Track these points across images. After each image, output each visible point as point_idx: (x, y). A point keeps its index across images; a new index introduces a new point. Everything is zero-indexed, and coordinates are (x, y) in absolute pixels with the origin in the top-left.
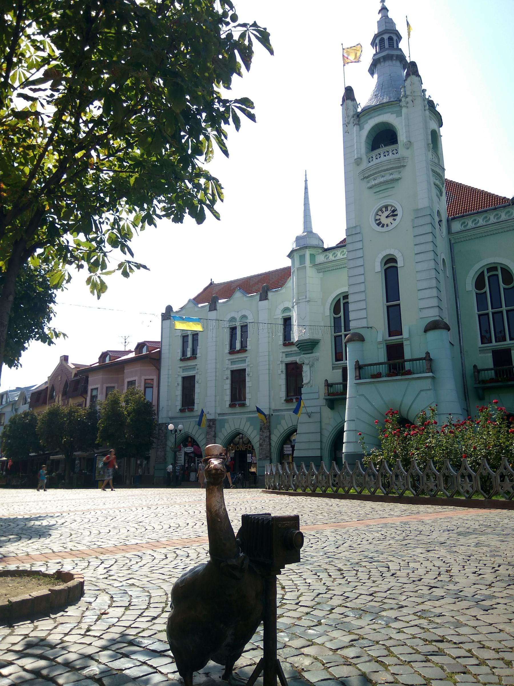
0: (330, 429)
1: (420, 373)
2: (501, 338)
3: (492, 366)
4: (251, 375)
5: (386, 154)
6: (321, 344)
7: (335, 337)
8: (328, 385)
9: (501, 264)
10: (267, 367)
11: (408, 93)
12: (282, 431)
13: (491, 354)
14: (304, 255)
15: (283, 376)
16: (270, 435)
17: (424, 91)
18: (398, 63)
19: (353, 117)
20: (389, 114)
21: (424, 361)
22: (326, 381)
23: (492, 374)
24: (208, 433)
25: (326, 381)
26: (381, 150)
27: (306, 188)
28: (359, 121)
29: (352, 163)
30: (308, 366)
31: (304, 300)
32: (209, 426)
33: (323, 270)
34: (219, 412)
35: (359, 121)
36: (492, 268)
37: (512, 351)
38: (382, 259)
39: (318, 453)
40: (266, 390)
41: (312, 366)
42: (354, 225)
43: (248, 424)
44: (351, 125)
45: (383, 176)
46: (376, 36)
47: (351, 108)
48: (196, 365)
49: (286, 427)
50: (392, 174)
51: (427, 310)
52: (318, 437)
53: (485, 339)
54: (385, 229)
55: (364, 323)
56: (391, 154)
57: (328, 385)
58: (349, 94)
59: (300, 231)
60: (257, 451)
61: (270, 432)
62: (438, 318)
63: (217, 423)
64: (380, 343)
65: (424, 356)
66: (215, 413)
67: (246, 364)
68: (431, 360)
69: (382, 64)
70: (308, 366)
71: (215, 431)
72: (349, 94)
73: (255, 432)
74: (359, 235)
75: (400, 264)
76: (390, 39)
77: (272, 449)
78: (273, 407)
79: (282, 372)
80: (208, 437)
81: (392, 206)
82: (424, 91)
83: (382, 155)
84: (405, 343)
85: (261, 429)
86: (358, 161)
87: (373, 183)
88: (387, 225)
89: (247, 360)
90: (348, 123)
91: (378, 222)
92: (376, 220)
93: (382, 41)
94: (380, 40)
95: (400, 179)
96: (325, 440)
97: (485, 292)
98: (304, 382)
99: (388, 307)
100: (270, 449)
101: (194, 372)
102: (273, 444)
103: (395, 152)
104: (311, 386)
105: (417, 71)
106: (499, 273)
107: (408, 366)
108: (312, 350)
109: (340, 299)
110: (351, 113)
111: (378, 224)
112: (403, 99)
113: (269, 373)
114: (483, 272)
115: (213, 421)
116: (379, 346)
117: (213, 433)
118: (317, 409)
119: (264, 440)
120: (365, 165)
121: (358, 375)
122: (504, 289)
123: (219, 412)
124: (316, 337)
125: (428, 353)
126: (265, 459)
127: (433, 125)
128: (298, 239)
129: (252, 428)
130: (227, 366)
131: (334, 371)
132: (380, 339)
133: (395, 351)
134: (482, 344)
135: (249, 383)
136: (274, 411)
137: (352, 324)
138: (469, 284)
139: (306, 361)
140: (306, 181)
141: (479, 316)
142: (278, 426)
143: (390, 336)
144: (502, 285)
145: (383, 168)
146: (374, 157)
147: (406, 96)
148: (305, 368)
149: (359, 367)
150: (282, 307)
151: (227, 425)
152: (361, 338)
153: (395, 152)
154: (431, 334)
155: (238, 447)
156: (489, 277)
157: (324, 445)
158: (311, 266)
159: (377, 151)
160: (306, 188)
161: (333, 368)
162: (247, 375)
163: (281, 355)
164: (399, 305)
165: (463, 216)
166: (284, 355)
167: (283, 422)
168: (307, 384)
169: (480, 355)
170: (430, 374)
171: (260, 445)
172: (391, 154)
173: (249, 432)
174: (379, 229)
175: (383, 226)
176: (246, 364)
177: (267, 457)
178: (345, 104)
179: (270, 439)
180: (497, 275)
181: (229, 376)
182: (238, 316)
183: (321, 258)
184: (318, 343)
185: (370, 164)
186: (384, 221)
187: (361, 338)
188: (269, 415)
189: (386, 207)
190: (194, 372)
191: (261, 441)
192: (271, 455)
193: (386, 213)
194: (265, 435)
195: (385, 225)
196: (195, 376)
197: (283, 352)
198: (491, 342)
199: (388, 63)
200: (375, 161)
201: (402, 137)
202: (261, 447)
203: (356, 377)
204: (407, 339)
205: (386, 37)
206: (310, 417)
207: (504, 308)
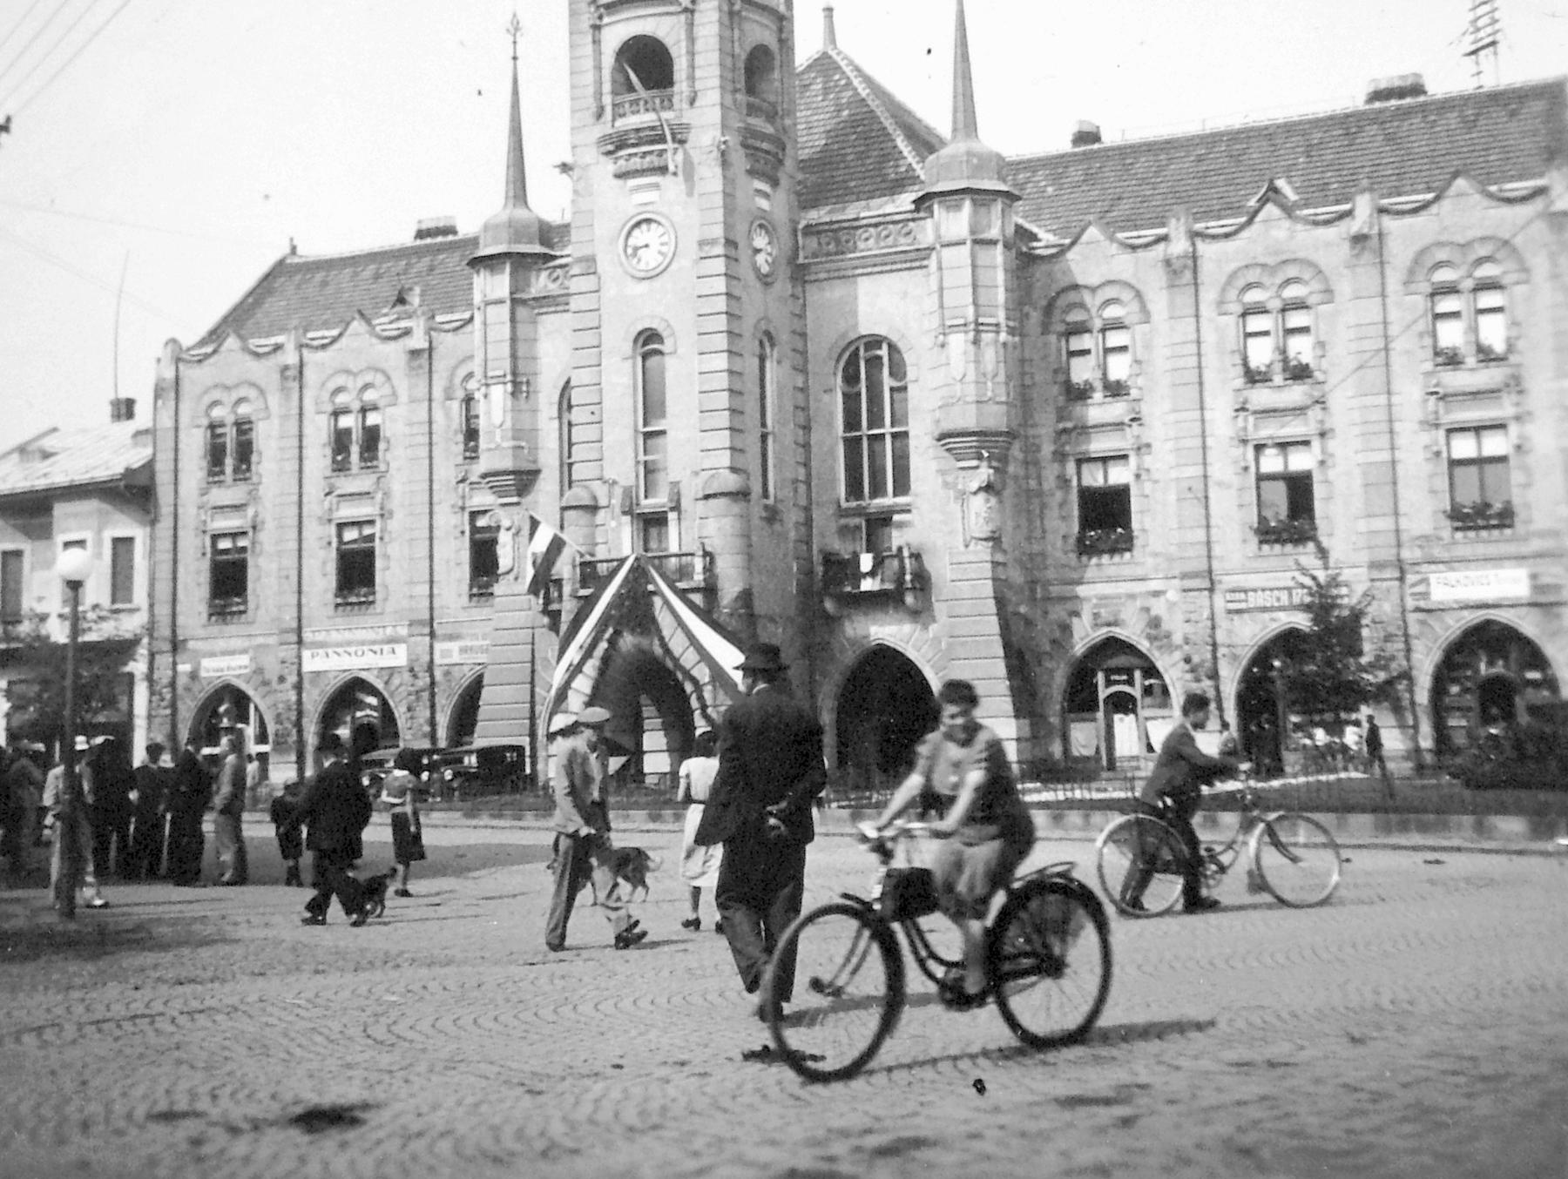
27: (515, 92)
30: (510, 533)
36: (874, 342)
53: (854, 489)
70: (510, 533)
75: (666, 347)
97: (859, 394)
98: (502, 569)
106: (884, 352)
122: (892, 389)
139: (505, 523)
144: (888, 382)
148: (504, 538)
160: (515, 92)
168: (508, 573)
171: (409, 709)
182: (353, 384)
207: (887, 429)
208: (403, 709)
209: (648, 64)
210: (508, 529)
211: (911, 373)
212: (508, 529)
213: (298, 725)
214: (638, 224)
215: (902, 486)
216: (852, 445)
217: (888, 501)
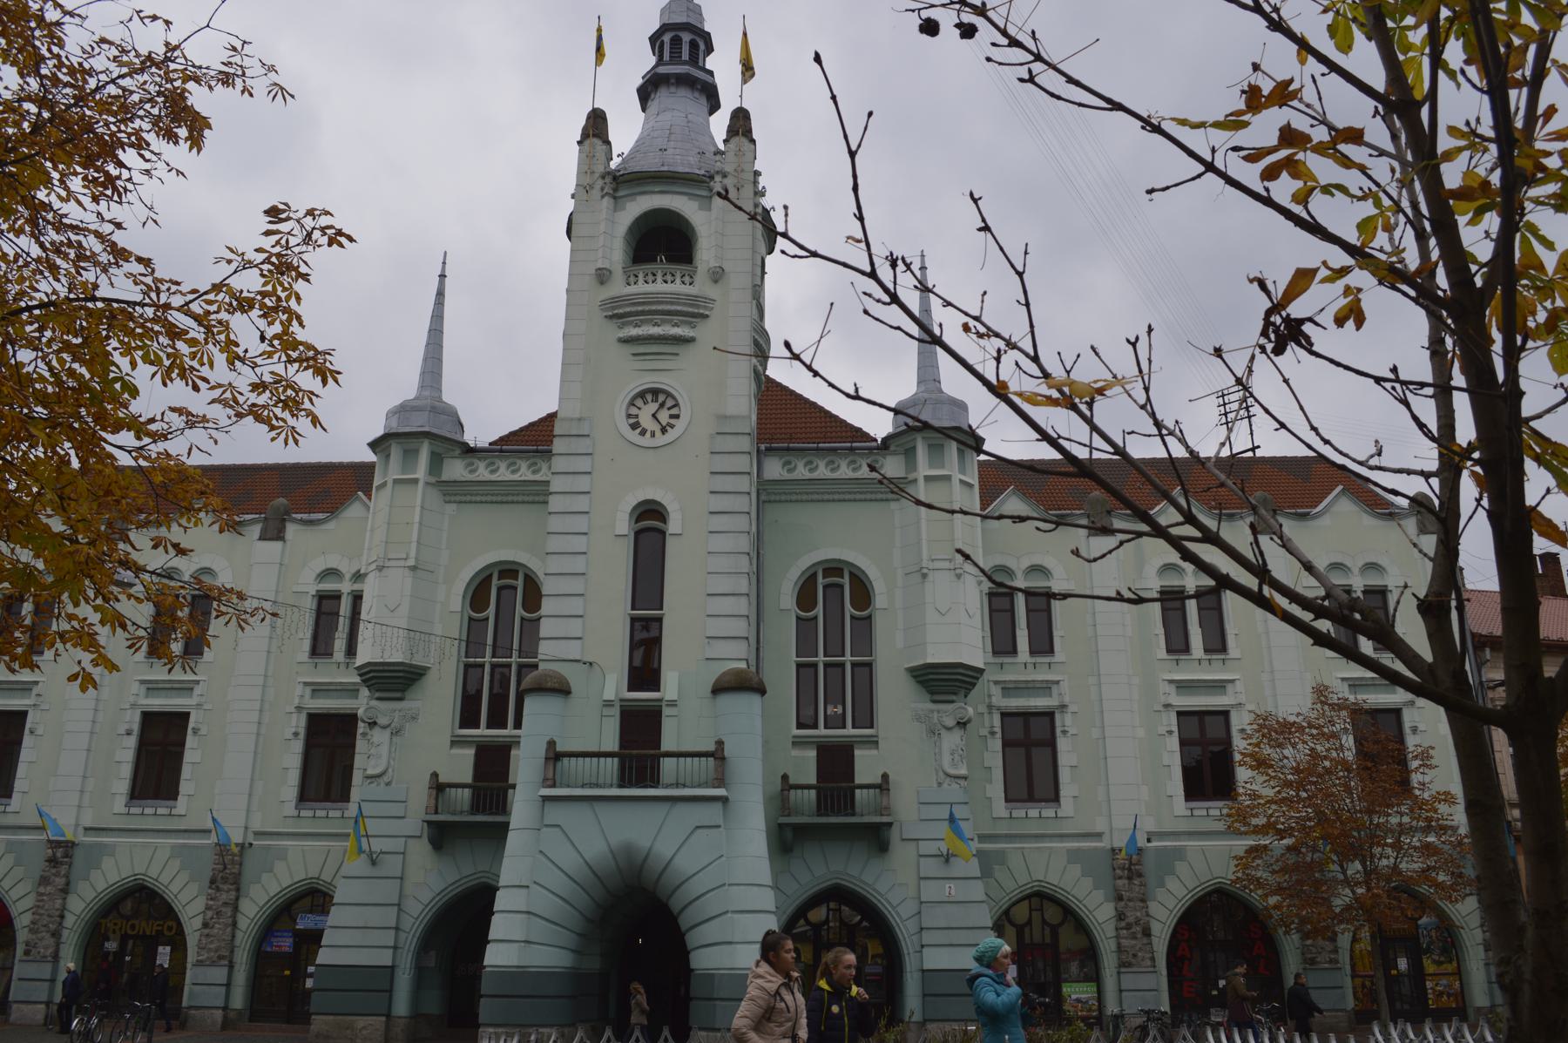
0: (426, 896)
1: (699, 786)
2: (837, 722)
3: (813, 780)
4: (203, 731)
5: (669, 278)
6: (430, 679)
7: (467, 666)
8: (439, 787)
9: (853, 565)
10: (255, 717)
11: (728, 168)
12: (274, 889)
13: (812, 754)
14: (417, 451)
15: (298, 746)
16: (237, 899)
17: (757, 174)
18: (704, 100)
19: (603, 177)
20: (685, 198)
21: (711, 759)
22: (435, 775)
23: (813, 793)
24: (44, 881)
25: (435, 775)
26: (661, 267)
27: (440, 294)
28: (615, 190)
29: (587, 276)
31: (402, 563)
32: (52, 861)
33: (458, 498)
34: (88, 821)
35: (615, 190)
36: (834, 569)
37: (857, 753)
38: (635, 508)
39: (385, 958)
40: (241, 775)
41: (396, 733)
42: (577, 415)
43: (176, 863)
44: (596, 193)
45: (656, 324)
46: (664, 28)
47: (601, 156)
48: (36, 683)
49: (286, 882)
50: (676, 325)
51: (722, 642)
52: (390, 916)
54: (646, 441)
55: (572, 650)
56: (678, 281)
57: (439, 787)
58: (596, 125)
59: (407, 387)
60: (192, 941)
61: (238, 890)
62: (743, 665)
63: (78, 855)
64: (608, 704)
65: (711, 747)
66: (77, 825)
67: (193, 701)
68: (723, 758)
69: (673, 89)
70: (388, 731)
71: (67, 876)
72: (596, 125)
73: (193, 889)
74: (587, 441)
75: (673, 526)
76: (694, 45)
77: (239, 935)
78: (257, 825)
79: (296, 734)
80: (42, 890)
81: (669, 395)
82: (757, 174)
83: (659, 279)
84: (666, 711)
85: (213, 881)
86: (602, 277)
87: (634, 332)
88: (653, 435)
89: (198, 690)
90: (592, 187)
91: (632, 421)
92: (629, 416)
93: (676, 41)
94: (672, 40)
95: (691, 340)
96: (407, 923)
97: (816, 618)
99: (634, 620)
100: (234, 937)
101: (27, 702)
102: (243, 923)
103: (687, 279)
104: (388, 784)
105: (750, 131)
106: (846, 581)
107: (667, 765)
108: (403, 691)
109: (491, 576)
110: (600, 169)
111: (634, 426)
112: (718, 178)
113: (258, 734)
114: (814, 575)
115: (69, 846)
116: (607, 711)
117: (60, 881)
118: (398, 845)
119: (218, 913)
120: (618, 288)
121: (550, 775)
122: (852, 617)
123: (88, 825)
124: (418, 661)
125: (720, 743)
126: (213, 964)
127: (763, 249)
128: (403, 410)
129: (184, 877)
130: (132, 699)
131: (456, 751)
132: (610, 694)
133: (640, 729)
134: (800, 726)
135: (192, 753)
136: (257, 834)
137: (545, 649)
138: (785, 596)
139: (382, 721)
140: (443, 276)
141: (799, 666)
142: (265, 877)
143: (630, 690)
145: (660, 307)
146: (641, 276)
147: (725, 176)
149: (554, 756)
150: (320, 565)
151: (107, 863)
152: (563, 690)
153: (687, 279)
154: (728, 701)
155: (133, 927)
156: (825, 587)
157: (403, 936)
158: (433, 480)
159: (649, 267)
160: (440, 294)
161: (454, 743)
162: (190, 731)
163: (299, 690)
164: (659, 620)
165: (788, 449)
166: (308, 690)
167: (280, 867)
168: (379, 776)
169: (795, 753)
170: (720, 792)
171: (205, 925)
172: (678, 281)
173: (174, 888)
174: (634, 436)
175: (643, 433)
176: (193, 701)
177: (221, 958)
178: (587, 142)
179: (236, 909)
180: (841, 587)
181: (136, 727)
183: (455, 469)
184: (422, 675)
185: (633, 289)
186: (646, 421)
187: (563, 690)
188: (242, 846)
189: (655, 392)
190: (27, 702)
191: (210, 914)
192: (232, 952)
193: (653, 407)
194: (224, 897)
195: (648, 434)
196: (24, 714)
197: (306, 684)
198: (815, 726)
199: (684, 92)
200: (641, 287)
201: (705, 254)
202: (206, 931)
203: (545, 779)
204: (672, 704)
205: (686, 37)
206: (374, 863)
207: (848, 658)
208: (198, 923)
209: (662, 242)
210: (384, 727)
211: (880, 600)
212: (384, 727)
213: (56, 935)
214: (642, 395)
215: (866, 715)
216: (805, 670)
217: (850, 731)
